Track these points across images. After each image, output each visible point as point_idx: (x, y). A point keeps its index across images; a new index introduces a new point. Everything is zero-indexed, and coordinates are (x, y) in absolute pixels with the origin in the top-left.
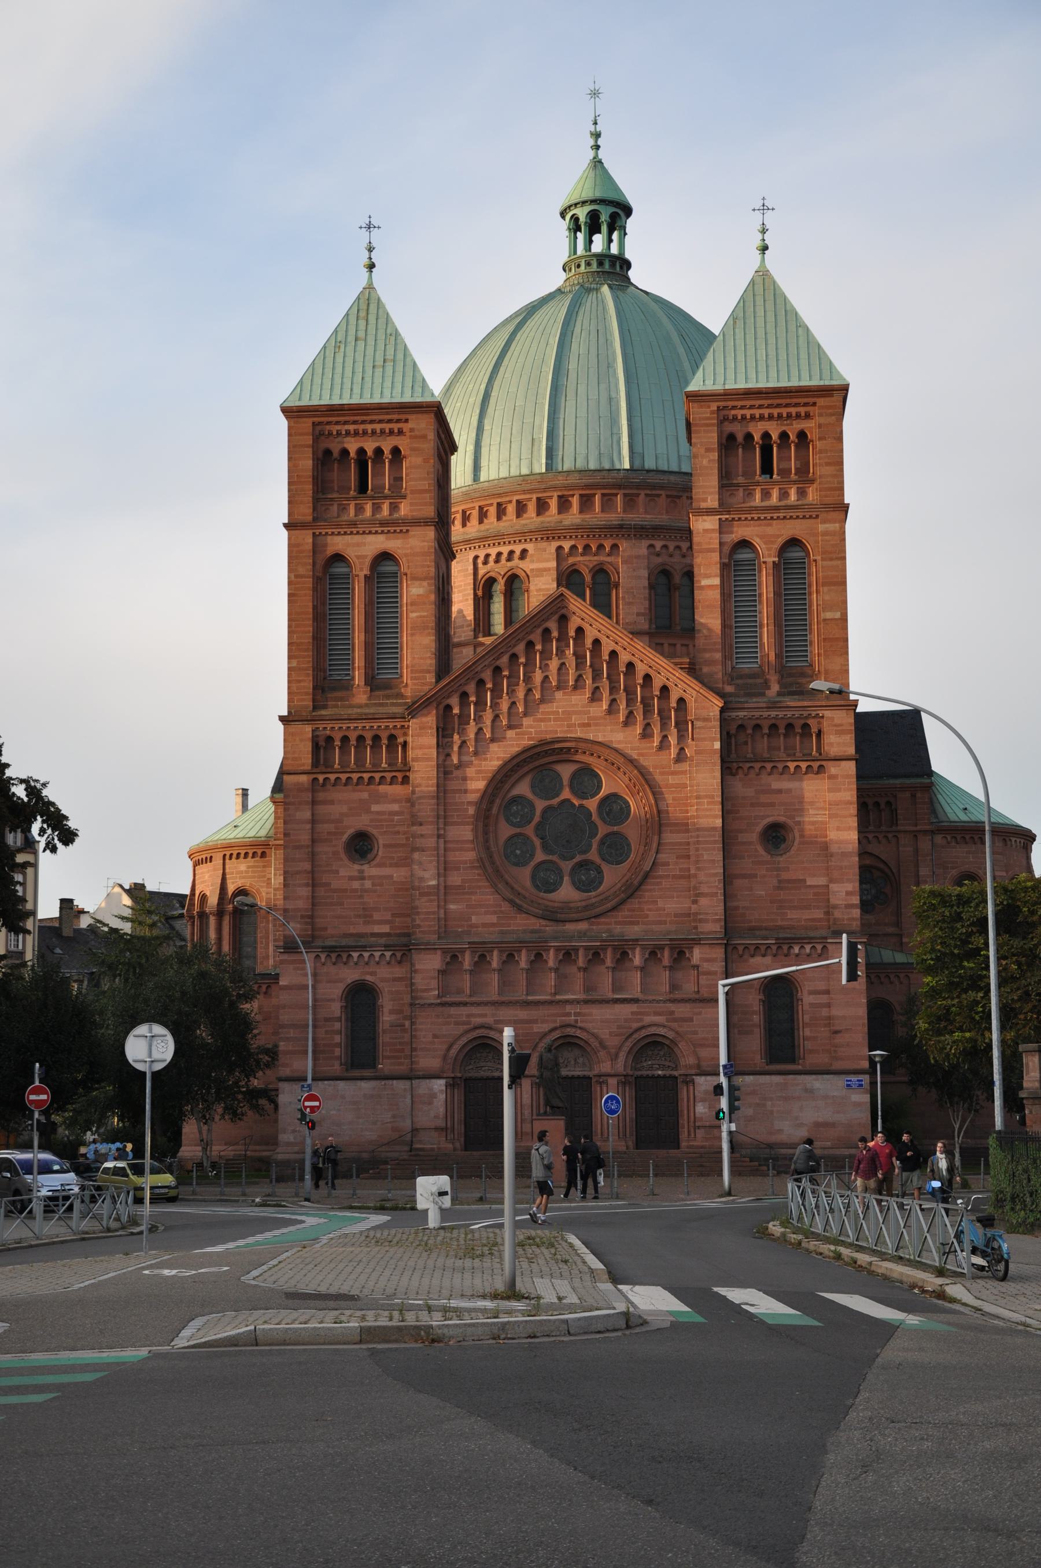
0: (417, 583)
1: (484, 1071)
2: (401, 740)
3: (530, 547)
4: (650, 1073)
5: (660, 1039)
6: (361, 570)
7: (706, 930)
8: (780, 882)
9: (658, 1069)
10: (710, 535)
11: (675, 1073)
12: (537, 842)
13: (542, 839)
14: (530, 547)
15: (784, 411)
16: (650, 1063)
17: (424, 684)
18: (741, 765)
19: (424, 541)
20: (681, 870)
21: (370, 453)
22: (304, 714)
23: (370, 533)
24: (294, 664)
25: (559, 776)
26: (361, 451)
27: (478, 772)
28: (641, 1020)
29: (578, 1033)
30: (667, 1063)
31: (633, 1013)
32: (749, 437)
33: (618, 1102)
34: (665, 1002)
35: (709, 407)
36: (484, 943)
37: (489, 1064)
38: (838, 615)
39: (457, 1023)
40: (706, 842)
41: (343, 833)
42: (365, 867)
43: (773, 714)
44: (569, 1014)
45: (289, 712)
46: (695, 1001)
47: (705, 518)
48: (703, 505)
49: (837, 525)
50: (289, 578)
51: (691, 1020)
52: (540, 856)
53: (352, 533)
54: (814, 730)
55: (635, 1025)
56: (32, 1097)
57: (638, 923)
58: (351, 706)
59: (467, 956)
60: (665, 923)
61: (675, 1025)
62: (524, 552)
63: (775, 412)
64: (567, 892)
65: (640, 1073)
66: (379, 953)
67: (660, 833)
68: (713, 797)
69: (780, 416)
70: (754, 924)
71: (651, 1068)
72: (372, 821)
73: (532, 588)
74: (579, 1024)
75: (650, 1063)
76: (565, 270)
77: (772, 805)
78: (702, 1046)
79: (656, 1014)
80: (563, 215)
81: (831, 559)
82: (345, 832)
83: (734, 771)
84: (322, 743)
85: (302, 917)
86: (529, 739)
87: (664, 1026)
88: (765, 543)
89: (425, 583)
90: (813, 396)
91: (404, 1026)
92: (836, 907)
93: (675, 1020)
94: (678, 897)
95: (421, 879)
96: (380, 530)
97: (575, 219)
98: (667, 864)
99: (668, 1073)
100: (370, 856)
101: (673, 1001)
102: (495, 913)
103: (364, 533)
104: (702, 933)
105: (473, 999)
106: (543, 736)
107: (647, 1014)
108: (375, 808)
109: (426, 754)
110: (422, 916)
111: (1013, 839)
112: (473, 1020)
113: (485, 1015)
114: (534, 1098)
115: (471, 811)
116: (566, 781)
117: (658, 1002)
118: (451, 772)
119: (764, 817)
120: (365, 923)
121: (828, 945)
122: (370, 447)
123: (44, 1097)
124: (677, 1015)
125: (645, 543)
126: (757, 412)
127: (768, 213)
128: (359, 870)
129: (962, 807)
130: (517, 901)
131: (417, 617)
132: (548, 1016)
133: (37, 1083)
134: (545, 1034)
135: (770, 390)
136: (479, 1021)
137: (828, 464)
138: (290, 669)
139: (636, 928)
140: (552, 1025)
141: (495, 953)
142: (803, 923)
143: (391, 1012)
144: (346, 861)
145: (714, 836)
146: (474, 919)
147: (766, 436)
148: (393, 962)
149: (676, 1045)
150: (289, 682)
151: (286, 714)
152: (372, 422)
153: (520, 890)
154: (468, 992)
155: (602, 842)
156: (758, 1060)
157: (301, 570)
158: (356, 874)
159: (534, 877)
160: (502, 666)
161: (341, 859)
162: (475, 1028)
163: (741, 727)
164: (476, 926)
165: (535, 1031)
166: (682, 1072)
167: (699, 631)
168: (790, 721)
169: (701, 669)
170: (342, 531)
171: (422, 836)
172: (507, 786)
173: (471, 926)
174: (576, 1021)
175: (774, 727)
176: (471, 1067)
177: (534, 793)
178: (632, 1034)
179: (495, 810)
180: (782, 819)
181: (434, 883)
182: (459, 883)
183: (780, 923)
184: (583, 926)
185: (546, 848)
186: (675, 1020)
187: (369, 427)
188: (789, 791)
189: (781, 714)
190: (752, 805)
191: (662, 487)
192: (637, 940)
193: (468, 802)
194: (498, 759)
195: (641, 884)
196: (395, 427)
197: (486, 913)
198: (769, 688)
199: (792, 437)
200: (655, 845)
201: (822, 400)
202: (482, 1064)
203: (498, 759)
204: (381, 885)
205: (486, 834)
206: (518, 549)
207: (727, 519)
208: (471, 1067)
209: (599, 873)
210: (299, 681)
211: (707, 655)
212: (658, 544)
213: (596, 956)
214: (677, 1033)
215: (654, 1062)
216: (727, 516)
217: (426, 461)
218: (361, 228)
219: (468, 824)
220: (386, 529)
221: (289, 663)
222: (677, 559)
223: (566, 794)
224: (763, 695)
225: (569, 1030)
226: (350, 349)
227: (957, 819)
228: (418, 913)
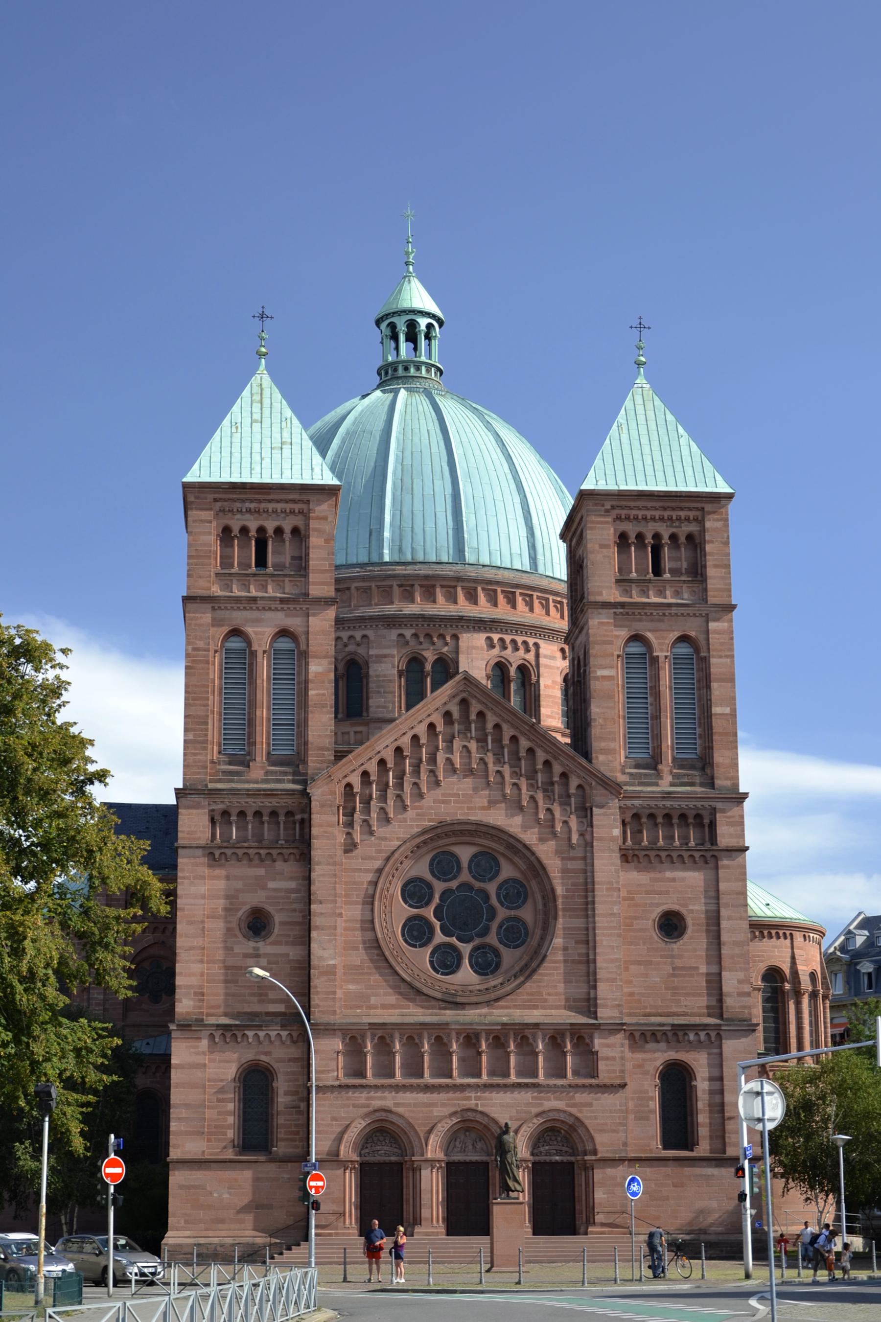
0: (317, 660)
2: (298, 817)
3: (370, 633)
4: (547, 1159)
6: (260, 645)
7: (605, 1016)
8: (674, 969)
10: (605, 628)
14: (370, 633)
15: (674, 514)
17: (322, 762)
18: (636, 853)
19: (325, 620)
21: (270, 531)
22: (200, 787)
23: (270, 609)
24: (191, 737)
26: (261, 530)
27: (379, 851)
28: (541, 1104)
29: (479, 1118)
30: (564, 1149)
32: (640, 537)
33: (639, 1184)
35: (603, 505)
37: (385, 1148)
38: (727, 710)
39: (354, 1106)
41: (238, 910)
42: (261, 944)
43: (668, 804)
44: (469, 1098)
45: (184, 785)
47: (600, 611)
48: (599, 599)
49: (726, 624)
50: (186, 650)
52: (440, 937)
53: (251, 608)
54: (706, 821)
55: (535, 1110)
56: (109, 1170)
57: (535, 1007)
58: (248, 782)
62: (364, 636)
63: (666, 514)
64: (466, 974)
65: (537, 1158)
66: (276, 1033)
68: (610, 883)
69: (670, 519)
70: (648, 1010)
71: (548, 1154)
72: (268, 898)
73: (371, 673)
74: (480, 1109)
75: (547, 1148)
76: (379, 374)
77: (667, 892)
78: (602, 1131)
80: (378, 323)
81: (721, 657)
82: (241, 909)
83: (630, 858)
84: (218, 818)
85: (195, 994)
86: (430, 820)
88: (657, 638)
89: (325, 662)
90: (701, 502)
91: (299, 1107)
92: (729, 995)
94: (576, 982)
95: (321, 958)
96: (280, 606)
97: (393, 326)
99: (565, 1159)
100: (263, 933)
103: (264, 608)
104: (601, 1018)
106: (442, 818)
107: (549, 1099)
108: (271, 885)
109: (325, 832)
110: (322, 996)
111: (811, 935)
116: (465, 864)
119: (658, 905)
120: (261, 1002)
121: (722, 1033)
122: (270, 526)
123: (118, 1170)
125: (483, 636)
126: (649, 514)
127: (644, 331)
128: (254, 948)
129: (765, 903)
130: (417, 984)
131: (317, 695)
132: (449, 1100)
133: (112, 1156)
135: (662, 494)
136: (378, 1104)
137: (715, 566)
138: (185, 741)
139: (536, 1012)
140: (453, 1109)
142: (696, 1010)
143: (286, 1093)
144: (241, 938)
146: (373, 1000)
147: (657, 536)
148: (288, 1043)
150: (185, 754)
151: (181, 787)
152: (270, 501)
155: (500, 927)
156: (656, 1146)
157: (200, 644)
158: (251, 951)
160: (403, 746)
161: (236, 936)
162: (375, 1111)
163: (636, 816)
167: (595, 719)
168: (683, 811)
169: (597, 757)
170: (242, 606)
171: (321, 914)
174: (477, 1105)
175: (668, 817)
176: (367, 1151)
177: (434, 875)
180: (675, 907)
181: (332, 962)
183: (674, 1010)
184: (485, 1010)
185: (445, 931)
186: (574, 1105)
187: (271, 506)
188: (683, 879)
189: (676, 804)
190: (647, 893)
191: (498, 583)
196: (297, 507)
197: (385, 994)
198: (661, 778)
199: (682, 539)
201: (710, 505)
202: (379, 1148)
204: (277, 963)
206: (358, 635)
207: (621, 613)
208: (367, 1151)
209: (496, 956)
210: (195, 754)
211: (603, 744)
212: (496, 637)
216: (622, 610)
217: (327, 541)
218: (254, 317)
220: (285, 606)
221: (185, 735)
222: (509, 652)
223: (465, 876)
224: (657, 785)
225: (469, 1114)
226: (246, 429)
227: (763, 915)
228: (317, 993)
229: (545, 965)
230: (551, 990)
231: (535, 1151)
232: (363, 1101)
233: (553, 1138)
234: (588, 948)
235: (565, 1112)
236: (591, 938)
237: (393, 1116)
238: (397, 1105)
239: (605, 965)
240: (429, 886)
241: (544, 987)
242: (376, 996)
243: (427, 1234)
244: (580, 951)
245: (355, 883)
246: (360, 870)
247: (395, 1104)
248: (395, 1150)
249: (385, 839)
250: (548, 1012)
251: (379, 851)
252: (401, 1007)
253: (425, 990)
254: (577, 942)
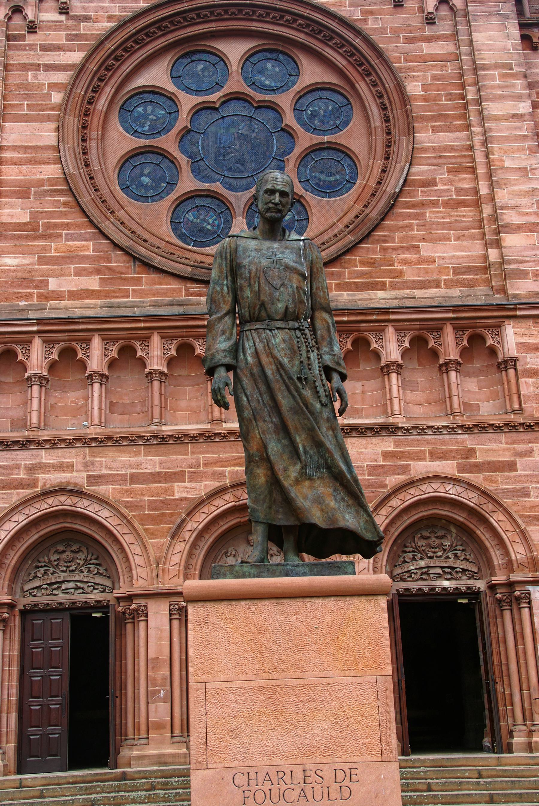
1: (66, 591)
4: (425, 585)
5: (444, 512)
9: (439, 576)
11: (481, 585)
12: (183, 160)
13: (190, 157)
16: (422, 563)
20: (458, 191)
25: (222, 59)
28: (405, 469)
30: (460, 565)
31: (386, 455)
34: (452, 430)
36: (71, 320)
37: (77, 576)
40: (507, 139)
46: (513, 428)
51: (511, 466)
55: (392, 481)
57: (382, 287)
59: (37, 344)
60: (437, 284)
61: (478, 479)
65: (402, 586)
67: (411, 131)
71: (425, 574)
75: (422, 563)
79: (436, 455)
87: (456, 481)
93: (477, 468)
94: (458, 238)
98: (432, 183)
101: (467, 429)
102: (98, 271)
104: (515, 296)
105: (46, 434)
107: (419, 457)
112: (42, 477)
113: (69, 467)
114: (176, 639)
115: (57, 97)
117: (437, 430)
118: (23, 37)
124: (480, 458)
132: (206, 465)
134: (201, 503)
139: (380, 294)
140: (217, 484)
141: (96, 342)
145: (519, 128)
146: (54, 284)
149: (484, 521)
153: (147, 236)
154: (35, 420)
159: (175, 224)
164: (58, 296)
165: (178, 495)
166: (499, 578)
172: (127, 67)
173: (47, 297)
176: (37, 583)
178: (387, 498)
179: (102, 104)
182: (26, 218)
186: (477, 468)
192: (386, 311)
193: (52, 86)
194: (110, 18)
195: (385, 216)
197: (78, 273)
200: (404, 153)
202: (62, 577)
203: (110, 18)
205: (84, 128)
208: (37, 583)
209: (299, 213)
213: (300, 351)
214: (484, 493)
215: (431, 563)
219: (49, 119)
229: (396, 211)
230: (407, 256)
231: (398, 571)
232: (22, 475)
233: (434, 542)
234: (477, 180)
235: (456, 481)
236: (480, 158)
237: (86, 503)
238: (93, 479)
239: (511, 201)
240: (172, 99)
241: (394, 249)
242: (61, 275)
243: (160, 760)
244: (460, 185)
245: (27, 86)
246: (36, 67)
247: (89, 477)
248: (98, 580)
249: (87, 18)
250: (406, 293)
251: (72, 38)
252: (108, 294)
253: (157, 261)
254: (451, 171)
